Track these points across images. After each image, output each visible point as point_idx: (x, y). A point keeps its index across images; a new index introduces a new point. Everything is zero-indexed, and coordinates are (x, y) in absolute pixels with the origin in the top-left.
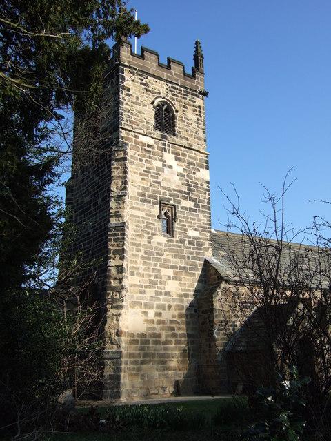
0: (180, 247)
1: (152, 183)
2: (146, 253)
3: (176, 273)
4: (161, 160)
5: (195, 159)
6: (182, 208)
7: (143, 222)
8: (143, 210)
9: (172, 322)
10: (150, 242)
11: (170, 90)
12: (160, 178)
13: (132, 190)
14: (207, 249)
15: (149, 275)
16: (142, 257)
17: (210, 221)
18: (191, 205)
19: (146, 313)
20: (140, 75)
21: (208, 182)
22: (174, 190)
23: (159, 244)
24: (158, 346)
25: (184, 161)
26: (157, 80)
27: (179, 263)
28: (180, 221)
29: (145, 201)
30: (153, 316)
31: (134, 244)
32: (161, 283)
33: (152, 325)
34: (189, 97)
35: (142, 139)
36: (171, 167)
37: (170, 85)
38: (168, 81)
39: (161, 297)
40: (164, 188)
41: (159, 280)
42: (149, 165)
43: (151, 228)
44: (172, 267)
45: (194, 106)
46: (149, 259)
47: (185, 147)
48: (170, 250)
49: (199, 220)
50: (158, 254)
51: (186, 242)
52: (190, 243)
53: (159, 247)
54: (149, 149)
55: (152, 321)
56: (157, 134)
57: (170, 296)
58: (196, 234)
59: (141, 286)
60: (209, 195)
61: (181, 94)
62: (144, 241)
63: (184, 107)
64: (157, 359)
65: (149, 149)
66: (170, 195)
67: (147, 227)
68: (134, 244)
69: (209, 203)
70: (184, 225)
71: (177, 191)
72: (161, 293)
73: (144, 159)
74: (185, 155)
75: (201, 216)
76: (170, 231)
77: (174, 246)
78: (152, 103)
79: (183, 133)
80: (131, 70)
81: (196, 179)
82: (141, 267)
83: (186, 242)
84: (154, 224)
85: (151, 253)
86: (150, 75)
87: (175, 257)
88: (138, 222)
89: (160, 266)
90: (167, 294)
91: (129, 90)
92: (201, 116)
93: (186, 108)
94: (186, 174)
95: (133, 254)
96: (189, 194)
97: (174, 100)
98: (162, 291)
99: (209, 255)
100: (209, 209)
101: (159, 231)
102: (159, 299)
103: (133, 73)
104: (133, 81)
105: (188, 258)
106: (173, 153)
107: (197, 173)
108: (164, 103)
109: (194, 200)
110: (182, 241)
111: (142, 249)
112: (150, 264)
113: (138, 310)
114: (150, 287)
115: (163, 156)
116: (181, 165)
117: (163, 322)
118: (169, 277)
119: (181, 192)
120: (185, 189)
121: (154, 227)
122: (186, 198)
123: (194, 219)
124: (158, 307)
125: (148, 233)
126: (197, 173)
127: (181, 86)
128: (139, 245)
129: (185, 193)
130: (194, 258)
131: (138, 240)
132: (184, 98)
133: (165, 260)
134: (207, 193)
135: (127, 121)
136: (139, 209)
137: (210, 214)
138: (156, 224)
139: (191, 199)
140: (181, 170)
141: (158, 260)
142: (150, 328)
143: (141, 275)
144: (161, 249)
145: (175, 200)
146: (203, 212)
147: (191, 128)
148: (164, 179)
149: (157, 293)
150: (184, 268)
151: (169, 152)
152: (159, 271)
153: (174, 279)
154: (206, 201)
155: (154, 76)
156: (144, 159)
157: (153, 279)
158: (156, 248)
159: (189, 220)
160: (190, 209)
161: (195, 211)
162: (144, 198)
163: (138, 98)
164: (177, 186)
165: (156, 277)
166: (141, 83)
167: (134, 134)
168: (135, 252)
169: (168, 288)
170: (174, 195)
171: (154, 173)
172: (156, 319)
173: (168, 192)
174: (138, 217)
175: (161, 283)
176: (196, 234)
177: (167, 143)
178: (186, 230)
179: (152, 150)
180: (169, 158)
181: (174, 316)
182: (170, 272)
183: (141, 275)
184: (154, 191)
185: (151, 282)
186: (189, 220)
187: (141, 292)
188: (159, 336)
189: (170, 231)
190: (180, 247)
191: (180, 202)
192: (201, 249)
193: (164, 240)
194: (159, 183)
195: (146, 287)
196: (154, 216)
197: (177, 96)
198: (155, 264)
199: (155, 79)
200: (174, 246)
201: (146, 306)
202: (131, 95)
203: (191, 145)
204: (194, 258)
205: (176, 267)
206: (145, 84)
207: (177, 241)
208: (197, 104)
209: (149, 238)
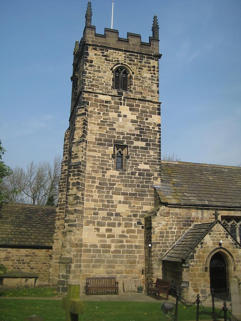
0: (131, 178)
1: (108, 130)
2: (100, 184)
3: (125, 198)
4: (116, 112)
5: (148, 108)
6: (134, 147)
7: (99, 160)
8: (99, 152)
9: (121, 236)
10: (104, 176)
11: (128, 57)
12: (115, 126)
13: (90, 137)
14: (156, 179)
15: (103, 201)
16: (97, 187)
17: (160, 156)
18: (143, 144)
19: (98, 230)
20: (101, 50)
21: (159, 125)
22: (127, 134)
23: (112, 176)
24: (107, 254)
25: (138, 111)
27: (130, 190)
28: (132, 157)
29: (101, 144)
30: (105, 232)
31: (91, 178)
32: (112, 206)
33: (102, 239)
34: (145, 60)
35: (101, 97)
36: (125, 116)
37: (128, 54)
38: (125, 51)
39: (112, 217)
40: (119, 133)
41: (111, 204)
43: (106, 165)
44: (123, 194)
45: (149, 67)
46: (103, 188)
47: (139, 100)
48: (122, 181)
49: (151, 156)
50: (110, 184)
51: (137, 174)
52: (140, 174)
53: (112, 179)
54: (107, 104)
55: (104, 236)
56: (115, 92)
57: (121, 216)
58: (147, 167)
59: (95, 209)
60: (160, 135)
61: (137, 59)
62: (100, 175)
63: (140, 68)
64: (106, 264)
65: (107, 104)
66: (123, 138)
67: (102, 164)
68: (91, 178)
69: (159, 142)
70: (136, 161)
71: (130, 134)
72: (112, 214)
73: (102, 113)
75: (152, 153)
77: (125, 177)
78: (112, 69)
79: (138, 89)
80: (94, 47)
81: (148, 123)
82: (96, 195)
83: (137, 174)
84: (108, 162)
85: (105, 184)
86: (111, 48)
87: (126, 186)
88: (95, 160)
89: (113, 194)
90: (118, 215)
91: (92, 62)
92: (154, 74)
93: (142, 69)
94: (139, 120)
95: (89, 185)
96: (141, 136)
97: (131, 64)
98: (114, 213)
99: (157, 183)
100: (160, 146)
101: (112, 167)
102: (111, 219)
103: (95, 49)
104: (96, 55)
105: (138, 186)
106: (127, 105)
107: (149, 118)
108: (121, 68)
109: (145, 140)
110: (133, 173)
111: (97, 181)
112: (103, 192)
113: (91, 227)
114: (102, 210)
115: (118, 109)
116: (135, 114)
117: (113, 236)
118: (120, 202)
119: (134, 135)
120: (138, 132)
121: (108, 164)
122: (137, 140)
123: (144, 156)
124: (109, 225)
125: (103, 168)
126: (149, 118)
127: (137, 53)
128: (94, 178)
129: (137, 135)
130: (143, 186)
131: (93, 174)
132: (140, 62)
133: (116, 189)
134: (158, 133)
135: (89, 85)
136: (96, 151)
137: (160, 150)
138: (110, 161)
139: (143, 140)
141: (111, 189)
142: (101, 241)
143: (95, 201)
144: (113, 181)
145: (128, 142)
146: (153, 149)
148: (120, 127)
149: (108, 214)
150: (134, 194)
151: (124, 105)
152: (112, 197)
153: (124, 203)
154: (157, 140)
155: (114, 49)
156: (102, 113)
157: (106, 203)
158: (109, 180)
159: (140, 157)
160: (142, 148)
161: (146, 149)
162: (100, 142)
163: (99, 67)
164: (130, 130)
165: (108, 201)
166: (103, 56)
167: (94, 95)
168: (91, 184)
169: (118, 210)
170: (127, 138)
171: (110, 122)
172: (107, 234)
173: (121, 136)
174: (95, 157)
175: (112, 206)
176: (147, 167)
177: (122, 98)
178: (138, 165)
179: (109, 105)
180: (124, 110)
181: (123, 232)
182: (122, 198)
183: (95, 201)
184: (110, 136)
185: (103, 205)
186: (140, 157)
187: (95, 214)
188: (109, 246)
190: (131, 178)
191: (132, 143)
192: (151, 179)
193: (117, 173)
194: (114, 129)
195: (99, 209)
196: (109, 155)
197: (134, 61)
198: (108, 192)
199: (114, 51)
200: (125, 177)
201: (99, 224)
202: (93, 66)
203: (145, 98)
204: (143, 186)
205: (126, 194)
206: (105, 56)
207: (128, 174)
208: (152, 65)
209: (103, 172)
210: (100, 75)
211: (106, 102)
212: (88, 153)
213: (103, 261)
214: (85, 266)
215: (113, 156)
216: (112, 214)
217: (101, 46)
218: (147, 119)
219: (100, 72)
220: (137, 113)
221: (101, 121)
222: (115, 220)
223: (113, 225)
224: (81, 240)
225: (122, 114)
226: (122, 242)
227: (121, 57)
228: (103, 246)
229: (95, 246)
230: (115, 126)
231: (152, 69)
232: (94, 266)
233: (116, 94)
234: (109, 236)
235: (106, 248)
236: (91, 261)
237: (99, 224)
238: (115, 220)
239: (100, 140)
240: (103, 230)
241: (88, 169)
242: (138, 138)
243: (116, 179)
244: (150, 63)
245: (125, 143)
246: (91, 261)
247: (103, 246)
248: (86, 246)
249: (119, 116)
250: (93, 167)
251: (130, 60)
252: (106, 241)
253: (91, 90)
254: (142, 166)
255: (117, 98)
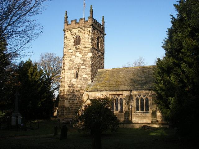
9: (77, 104)
12: (74, 62)
13: (66, 68)
18: (84, 67)
19: (69, 102)
23: (73, 81)
26: (75, 29)
31: (66, 83)
33: (71, 105)
34: (86, 29)
36: (78, 57)
37: (79, 29)
38: (78, 28)
42: (71, 59)
49: (87, 71)
55: (71, 104)
58: (86, 76)
68: (66, 83)
74: (83, 51)
76: (77, 77)
79: (83, 43)
83: (82, 79)
86: (73, 29)
91: (67, 37)
103: (68, 31)
105: (83, 84)
107: (87, 55)
110: (81, 79)
117: (74, 104)
119: (81, 64)
120: (82, 62)
122: (82, 65)
123: (85, 71)
124: (73, 100)
125: (70, 79)
126: (87, 55)
127: (83, 27)
130: (84, 84)
140: (81, 56)
142: (70, 106)
146: (88, 68)
147: (86, 40)
176: (86, 76)
177: (77, 49)
178: (82, 75)
180: (78, 54)
181: (77, 102)
184: (72, 66)
188: (73, 107)
189: (77, 77)
193: (75, 80)
194: (74, 63)
206: (71, 33)
210: (69, 41)
211: (71, 52)
212: (66, 74)
213: (71, 113)
214: (65, 114)
215: (74, 73)
216: (73, 96)
217: (69, 29)
218: (86, 56)
219: (69, 40)
220: (82, 54)
221: (70, 61)
222: (75, 98)
223: (74, 100)
224: (64, 105)
225: (77, 56)
226: (77, 106)
227: (76, 31)
228: (71, 107)
229: (68, 107)
230: (74, 62)
231: (89, 32)
232: (68, 114)
233: (75, 48)
234: (73, 104)
235: (72, 108)
236: (67, 113)
237: (70, 99)
238: (75, 98)
239: (69, 68)
240: (71, 101)
241: (66, 80)
242: (83, 64)
243: (75, 82)
244: (88, 30)
245: (78, 68)
246: (67, 113)
247: (71, 107)
248: (66, 107)
249: (76, 57)
250: (67, 79)
251: (80, 31)
252: (71, 106)
253: (66, 49)
254: (84, 76)
255: (75, 50)
